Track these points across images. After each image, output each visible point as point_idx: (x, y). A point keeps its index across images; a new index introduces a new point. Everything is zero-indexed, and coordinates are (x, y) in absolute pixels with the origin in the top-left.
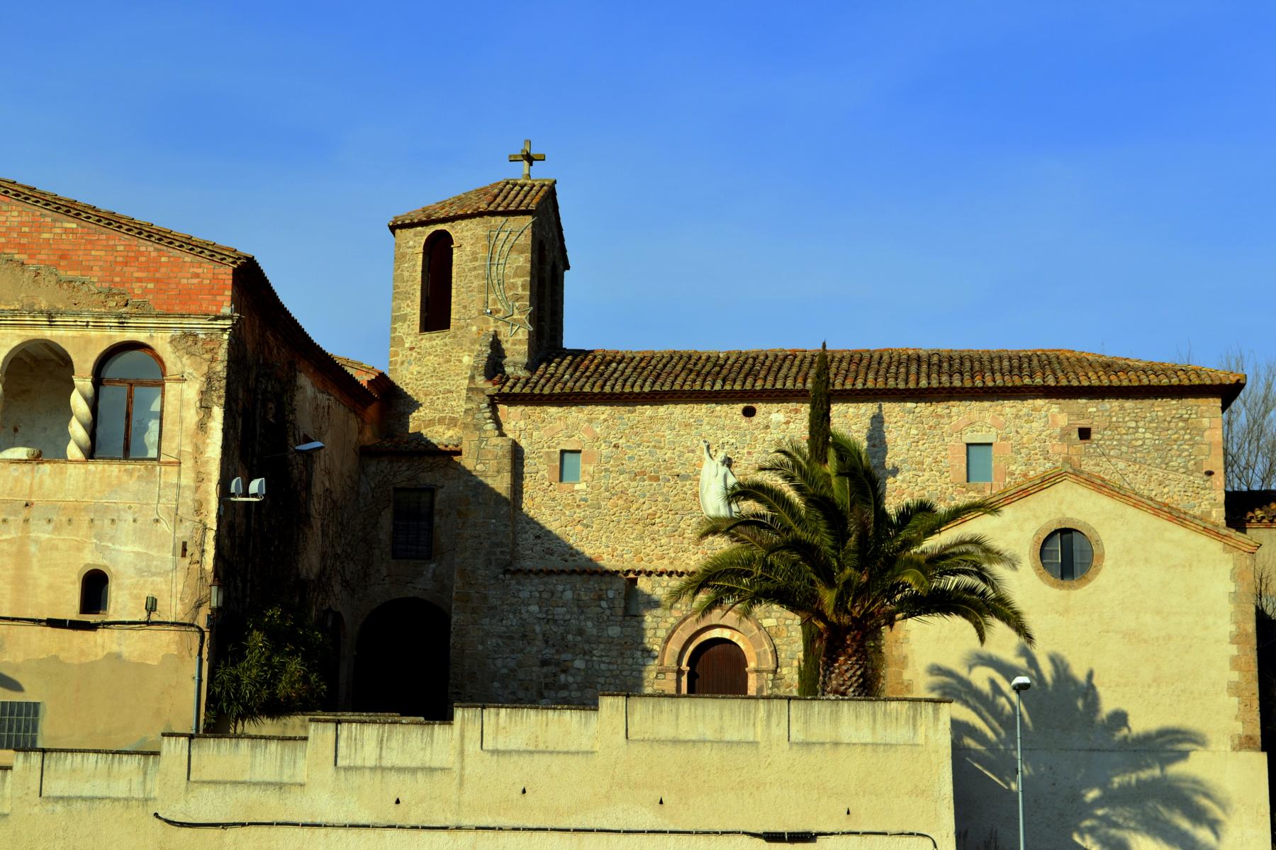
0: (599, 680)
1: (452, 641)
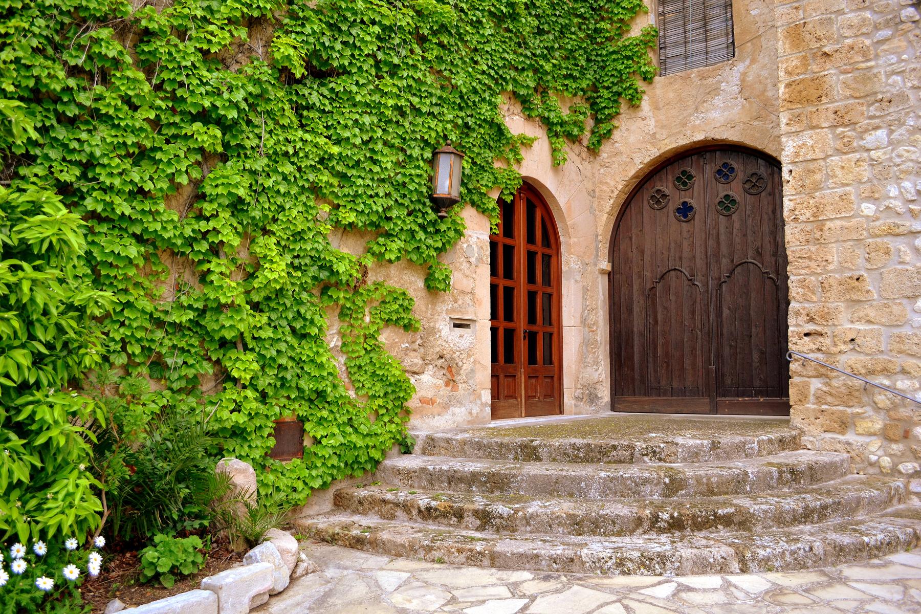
1: (787, 204)
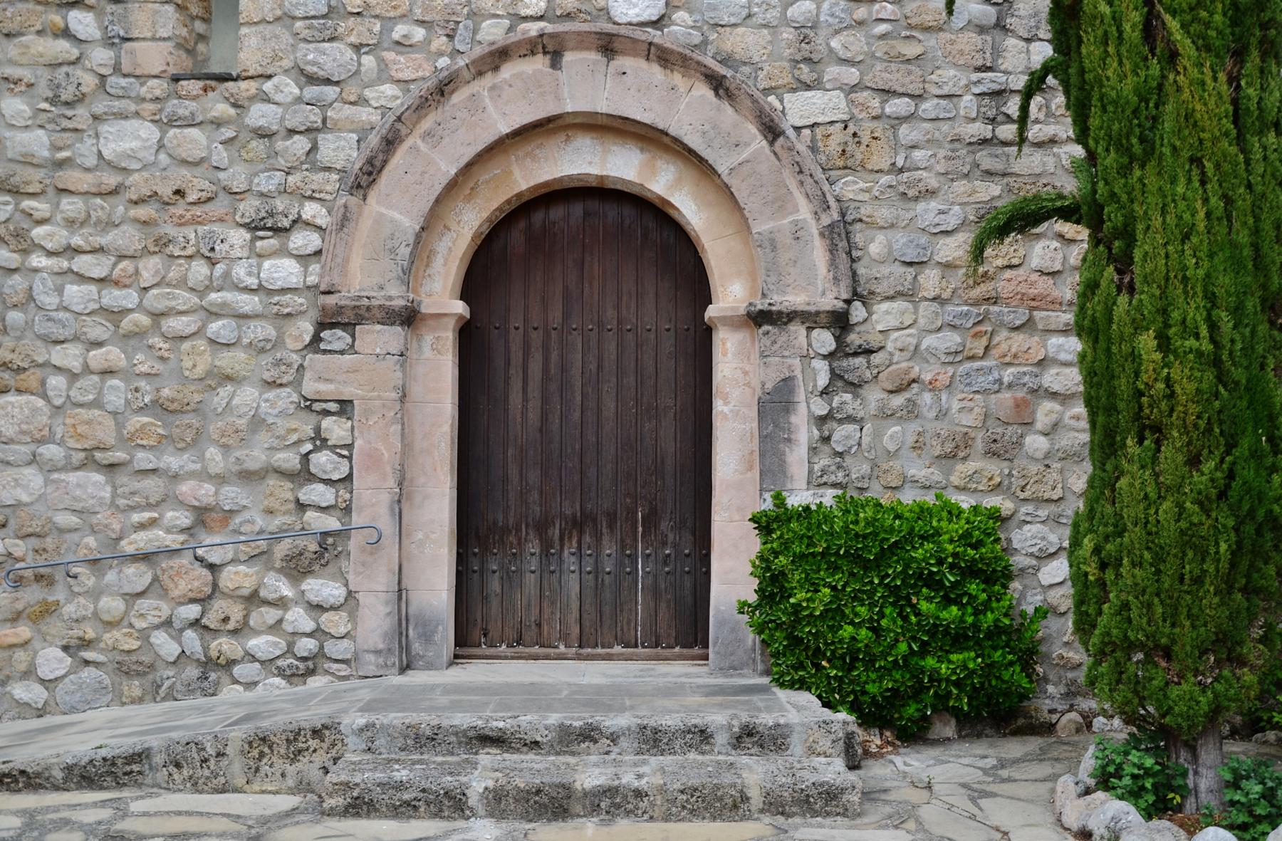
0: (58, 356)
